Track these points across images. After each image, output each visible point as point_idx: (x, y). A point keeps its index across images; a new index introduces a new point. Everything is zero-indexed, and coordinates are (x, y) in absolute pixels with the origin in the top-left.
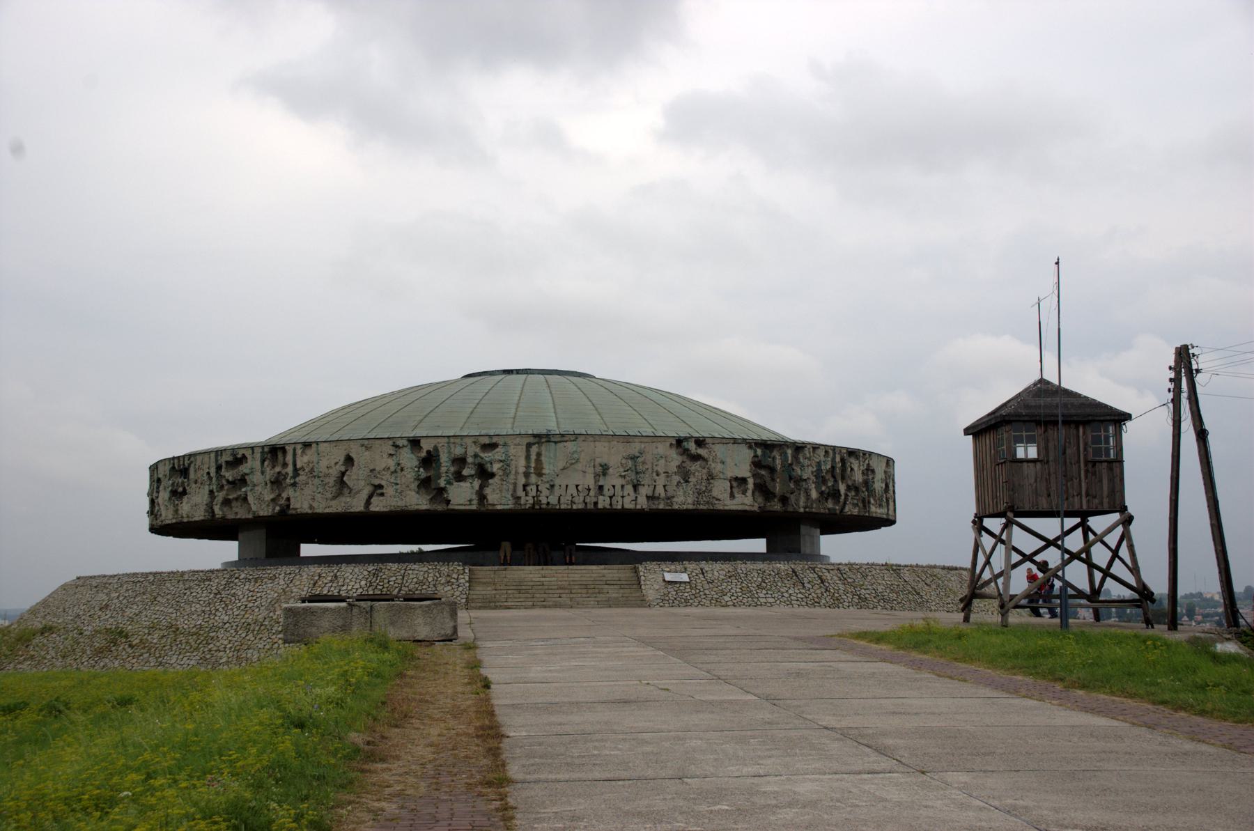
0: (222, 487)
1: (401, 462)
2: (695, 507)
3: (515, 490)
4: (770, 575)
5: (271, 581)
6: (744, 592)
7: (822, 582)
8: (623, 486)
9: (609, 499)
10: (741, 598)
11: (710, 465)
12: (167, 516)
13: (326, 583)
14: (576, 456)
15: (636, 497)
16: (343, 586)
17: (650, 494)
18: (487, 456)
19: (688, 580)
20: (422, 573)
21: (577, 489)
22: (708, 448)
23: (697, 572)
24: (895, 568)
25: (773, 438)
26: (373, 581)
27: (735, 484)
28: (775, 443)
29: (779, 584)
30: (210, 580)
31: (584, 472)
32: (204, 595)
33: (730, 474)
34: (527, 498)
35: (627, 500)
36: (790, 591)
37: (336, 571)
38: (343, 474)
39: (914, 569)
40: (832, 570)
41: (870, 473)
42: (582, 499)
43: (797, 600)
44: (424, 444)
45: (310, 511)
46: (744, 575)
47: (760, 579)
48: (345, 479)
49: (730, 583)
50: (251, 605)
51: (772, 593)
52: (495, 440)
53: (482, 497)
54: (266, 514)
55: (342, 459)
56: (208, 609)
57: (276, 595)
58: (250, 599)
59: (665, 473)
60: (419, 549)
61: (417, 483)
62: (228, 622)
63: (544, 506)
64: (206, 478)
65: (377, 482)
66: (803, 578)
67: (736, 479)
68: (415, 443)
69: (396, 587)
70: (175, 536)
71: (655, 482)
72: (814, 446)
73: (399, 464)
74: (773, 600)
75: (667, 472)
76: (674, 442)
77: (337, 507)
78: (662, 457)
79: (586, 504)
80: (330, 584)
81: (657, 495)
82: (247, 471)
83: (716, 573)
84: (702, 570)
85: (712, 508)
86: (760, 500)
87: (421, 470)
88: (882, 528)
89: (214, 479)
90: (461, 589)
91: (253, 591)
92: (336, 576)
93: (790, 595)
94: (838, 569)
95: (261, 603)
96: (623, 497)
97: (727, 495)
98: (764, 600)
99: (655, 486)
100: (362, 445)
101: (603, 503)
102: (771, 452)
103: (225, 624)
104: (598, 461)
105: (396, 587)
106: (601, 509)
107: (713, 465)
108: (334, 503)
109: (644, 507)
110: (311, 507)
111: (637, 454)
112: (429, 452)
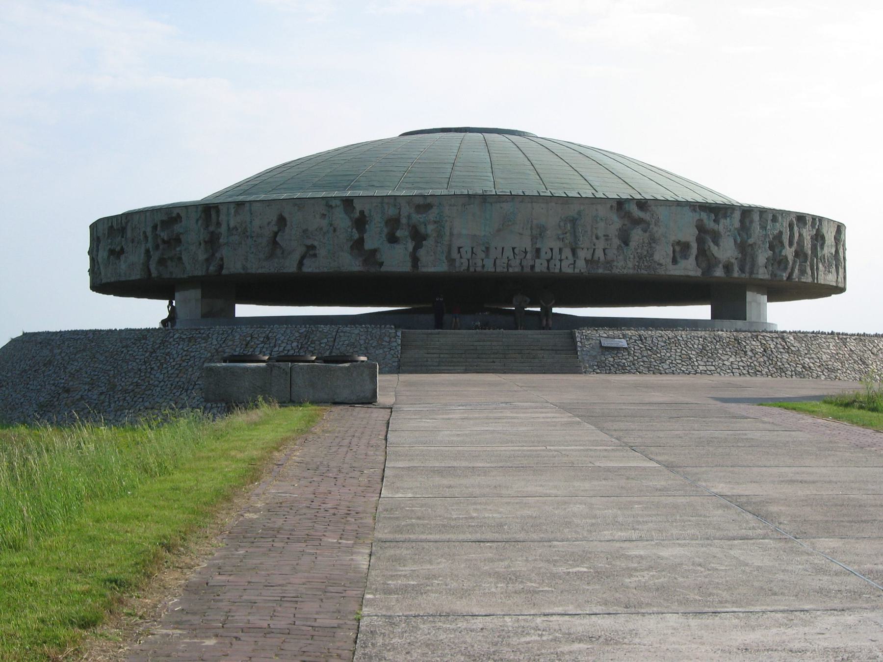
0: (157, 247)
1: (333, 222)
3: (449, 252)
5: (203, 341)
8: (560, 250)
9: (546, 263)
10: (680, 366)
11: (653, 228)
12: (107, 276)
13: (259, 344)
15: (575, 261)
16: (275, 346)
17: (589, 257)
19: (626, 346)
24: (841, 336)
25: (719, 200)
26: (305, 342)
27: (678, 249)
28: (721, 206)
30: (146, 339)
32: (140, 353)
33: (673, 238)
34: (462, 261)
36: (731, 360)
37: (268, 332)
38: (276, 234)
40: (777, 338)
41: (819, 238)
42: (518, 262)
43: (739, 369)
44: (358, 206)
45: (242, 271)
47: (700, 347)
50: (185, 364)
52: (429, 200)
53: (415, 260)
54: (200, 274)
55: (275, 219)
56: (144, 367)
58: (184, 358)
59: (604, 236)
61: (351, 243)
62: (162, 381)
63: (479, 269)
64: (142, 237)
65: (309, 242)
67: (679, 243)
68: (348, 202)
70: (115, 295)
71: (594, 245)
72: (761, 210)
73: (331, 225)
74: (713, 368)
75: (607, 236)
76: (615, 205)
79: (522, 267)
80: (261, 345)
82: (181, 231)
84: (640, 336)
85: (653, 272)
87: (354, 230)
88: (833, 295)
89: (150, 239)
90: (392, 352)
91: (187, 350)
92: (268, 338)
95: (194, 363)
96: (561, 260)
97: (669, 260)
99: (594, 250)
101: (540, 267)
103: (160, 382)
104: (535, 222)
106: (538, 273)
107: (655, 229)
109: (582, 271)
110: (244, 268)
111: (576, 216)
112: (362, 212)
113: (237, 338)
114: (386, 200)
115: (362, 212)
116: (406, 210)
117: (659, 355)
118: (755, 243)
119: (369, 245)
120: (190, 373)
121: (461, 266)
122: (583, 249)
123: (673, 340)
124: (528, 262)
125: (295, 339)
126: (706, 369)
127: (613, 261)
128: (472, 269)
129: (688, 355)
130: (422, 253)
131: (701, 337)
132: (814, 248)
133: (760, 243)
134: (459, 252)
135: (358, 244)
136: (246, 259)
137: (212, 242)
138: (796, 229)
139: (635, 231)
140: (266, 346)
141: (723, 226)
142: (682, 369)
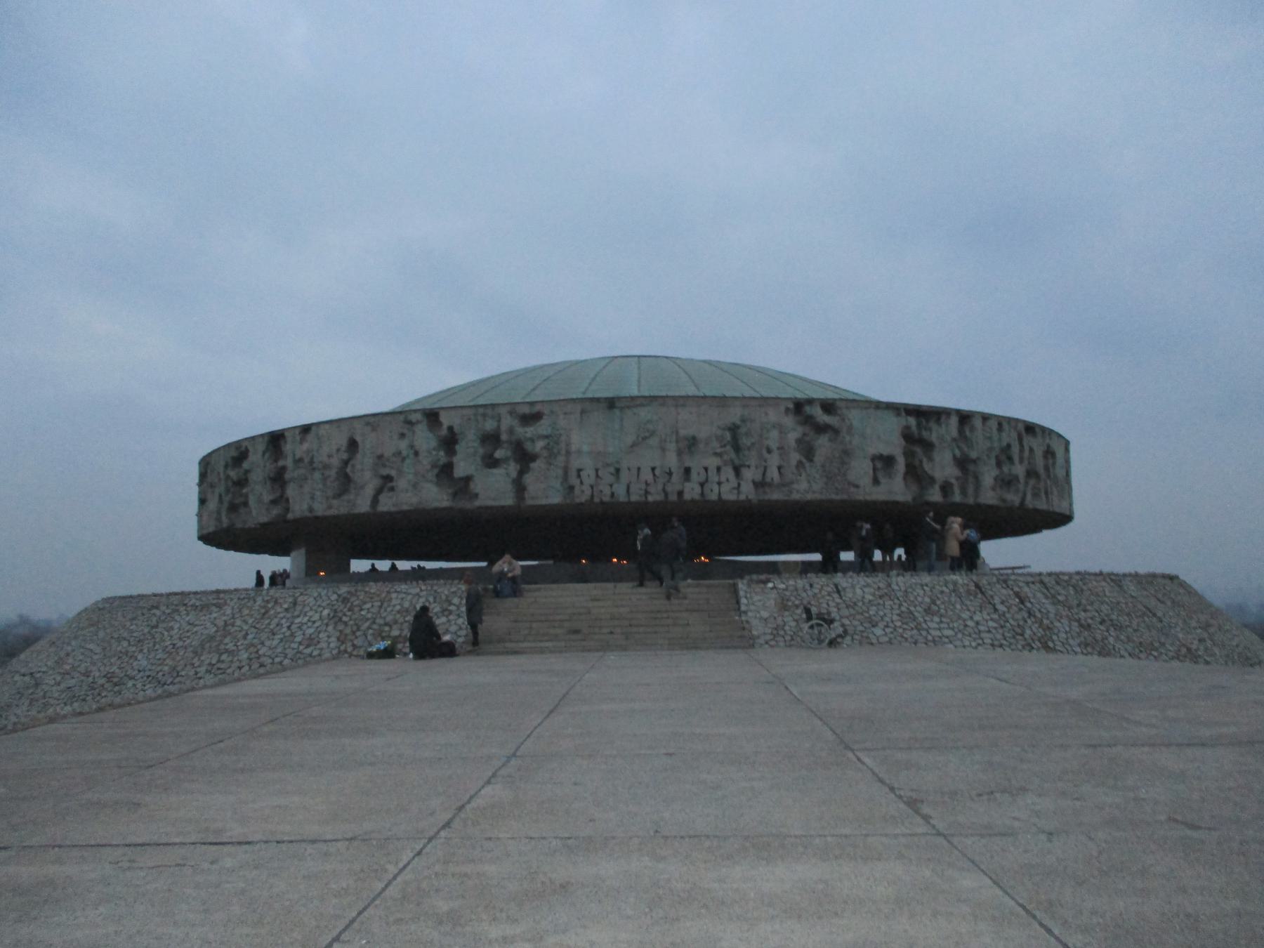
0: (228, 491)
2: (823, 497)
4: (942, 592)
6: (905, 621)
7: (1022, 602)
8: (719, 469)
10: (901, 631)
13: (279, 613)
14: (650, 427)
16: (298, 616)
17: (758, 478)
18: (530, 431)
20: (409, 597)
21: (654, 475)
22: (840, 415)
23: (829, 589)
24: (1113, 577)
27: (879, 465)
29: (958, 606)
31: (663, 450)
35: (725, 488)
36: (977, 618)
38: (346, 463)
39: (1136, 576)
40: (1033, 583)
42: (660, 487)
43: (989, 632)
44: (445, 420)
46: (901, 594)
47: (927, 600)
48: (348, 470)
49: (881, 607)
50: (180, 644)
51: (948, 620)
52: (537, 408)
53: (520, 487)
56: (134, 649)
57: (215, 629)
59: (778, 448)
60: (419, 566)
61: (436, 471)
63: (606, 499)
65: (385, 472)
66: (992, 597)
68: (432, 416)
69: (368, 619)
71: (765, 461)
73: (412, 447)
76: (791, 406)
77: (339, 508)
78: (774, 427)
79: (666, 494)
80: (281, 615)
81: (768, 480)
83: (859, 591)
84: (836, 586)
86: (914, 488)
87: (442, 453)
93: (977, 623)
94: (1042, 582)
96: (719, 483)
97: (866, 481)
98: (938, 633)
99: (765, 468)
100: (368, 424)
101: (692, 491)
102: (927, 421)
103: (139, 671)
104: (683, 432)
105: (368, 619)
107: (848, 438)
108: (335, 502)
109: (750, 497)
110: (311, 510)
111: (738, 423)
112: (450, 429)
113: (258, 603)
114: (481, 410)
115: (450, 429)
116: (507, 422)
117: (867, 615)
118: (978, 458)
119: (461, 470)
120: (178, 658)
121: (583, 495)
122: (749, 467)
123: (886, 591)
124: (673, 488)
125: (328, 604)
126: (940, 635)
127: (792, 483)
128: (596, 500)
129: (911, 612)
130: (528, 479)
131: (927, 585)
132: (1047, 468)
133: (985, 457)
134: (579, 476)
135: (445, 472)
136: (312, 498)
137: (278, 479)
138: (1025, 444)
139: (820, 441)
140: (289, 615)
141: (935, 433)
142: (905, 635)
